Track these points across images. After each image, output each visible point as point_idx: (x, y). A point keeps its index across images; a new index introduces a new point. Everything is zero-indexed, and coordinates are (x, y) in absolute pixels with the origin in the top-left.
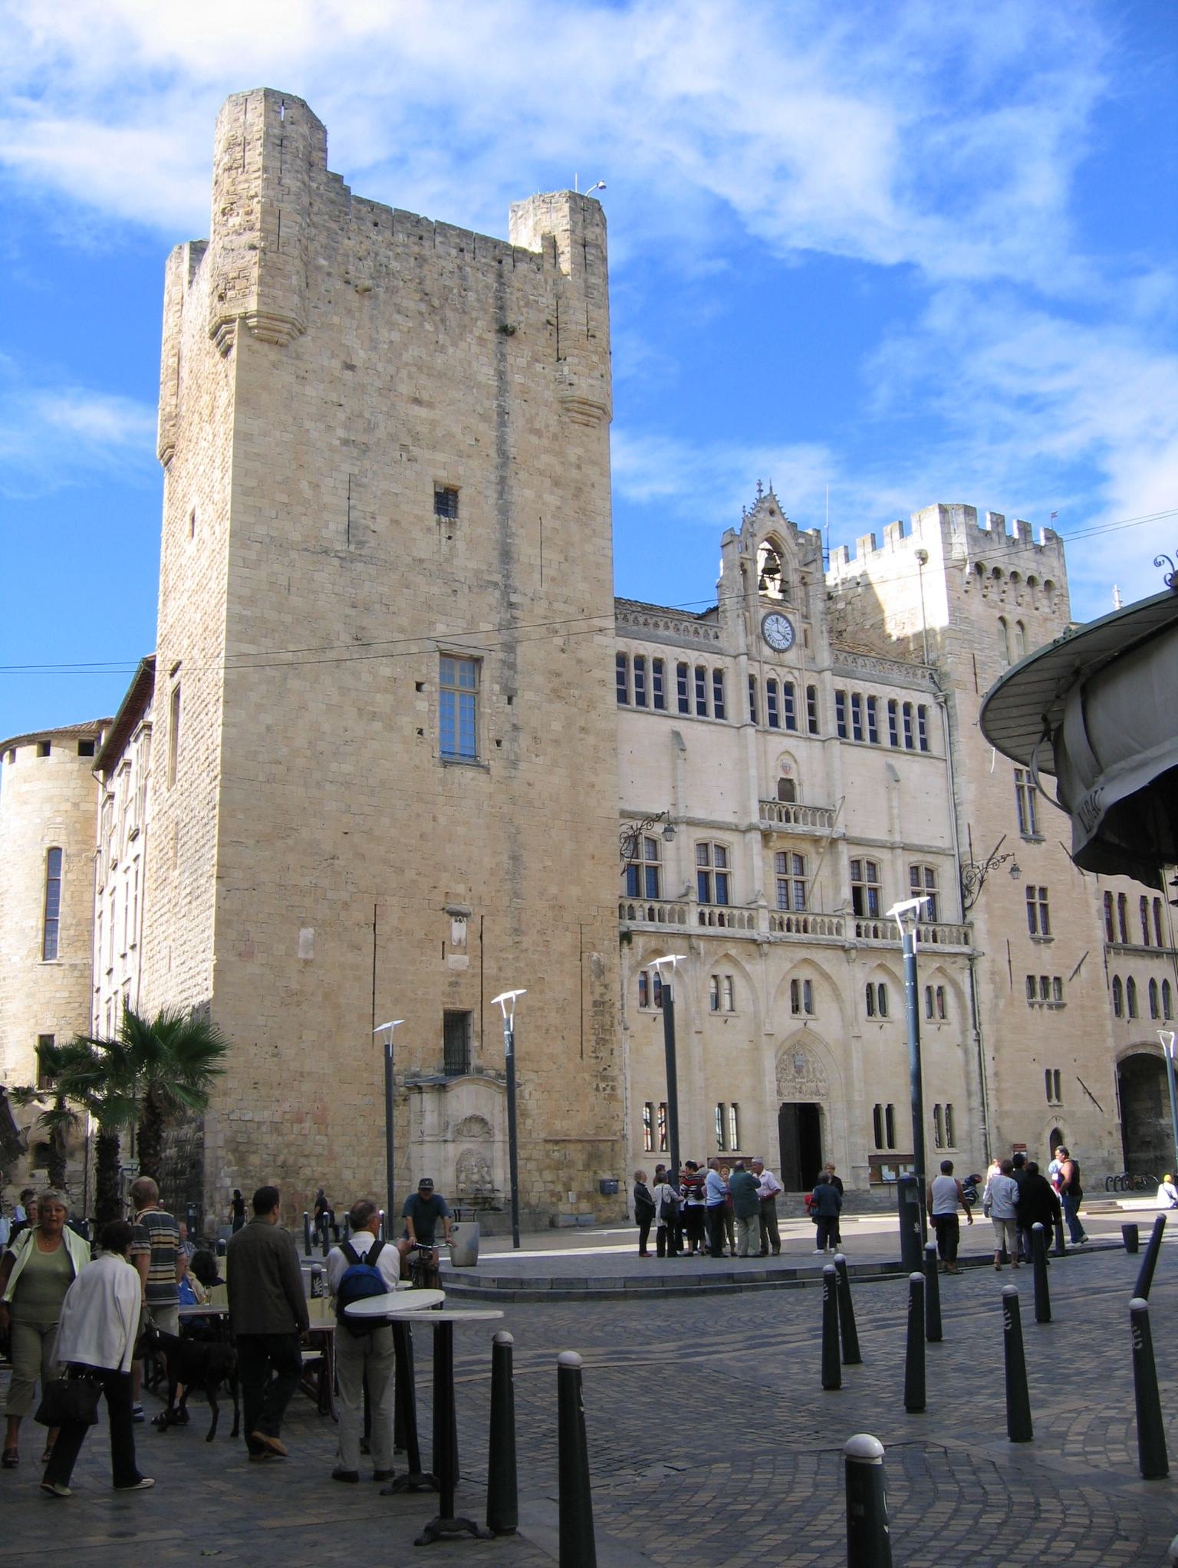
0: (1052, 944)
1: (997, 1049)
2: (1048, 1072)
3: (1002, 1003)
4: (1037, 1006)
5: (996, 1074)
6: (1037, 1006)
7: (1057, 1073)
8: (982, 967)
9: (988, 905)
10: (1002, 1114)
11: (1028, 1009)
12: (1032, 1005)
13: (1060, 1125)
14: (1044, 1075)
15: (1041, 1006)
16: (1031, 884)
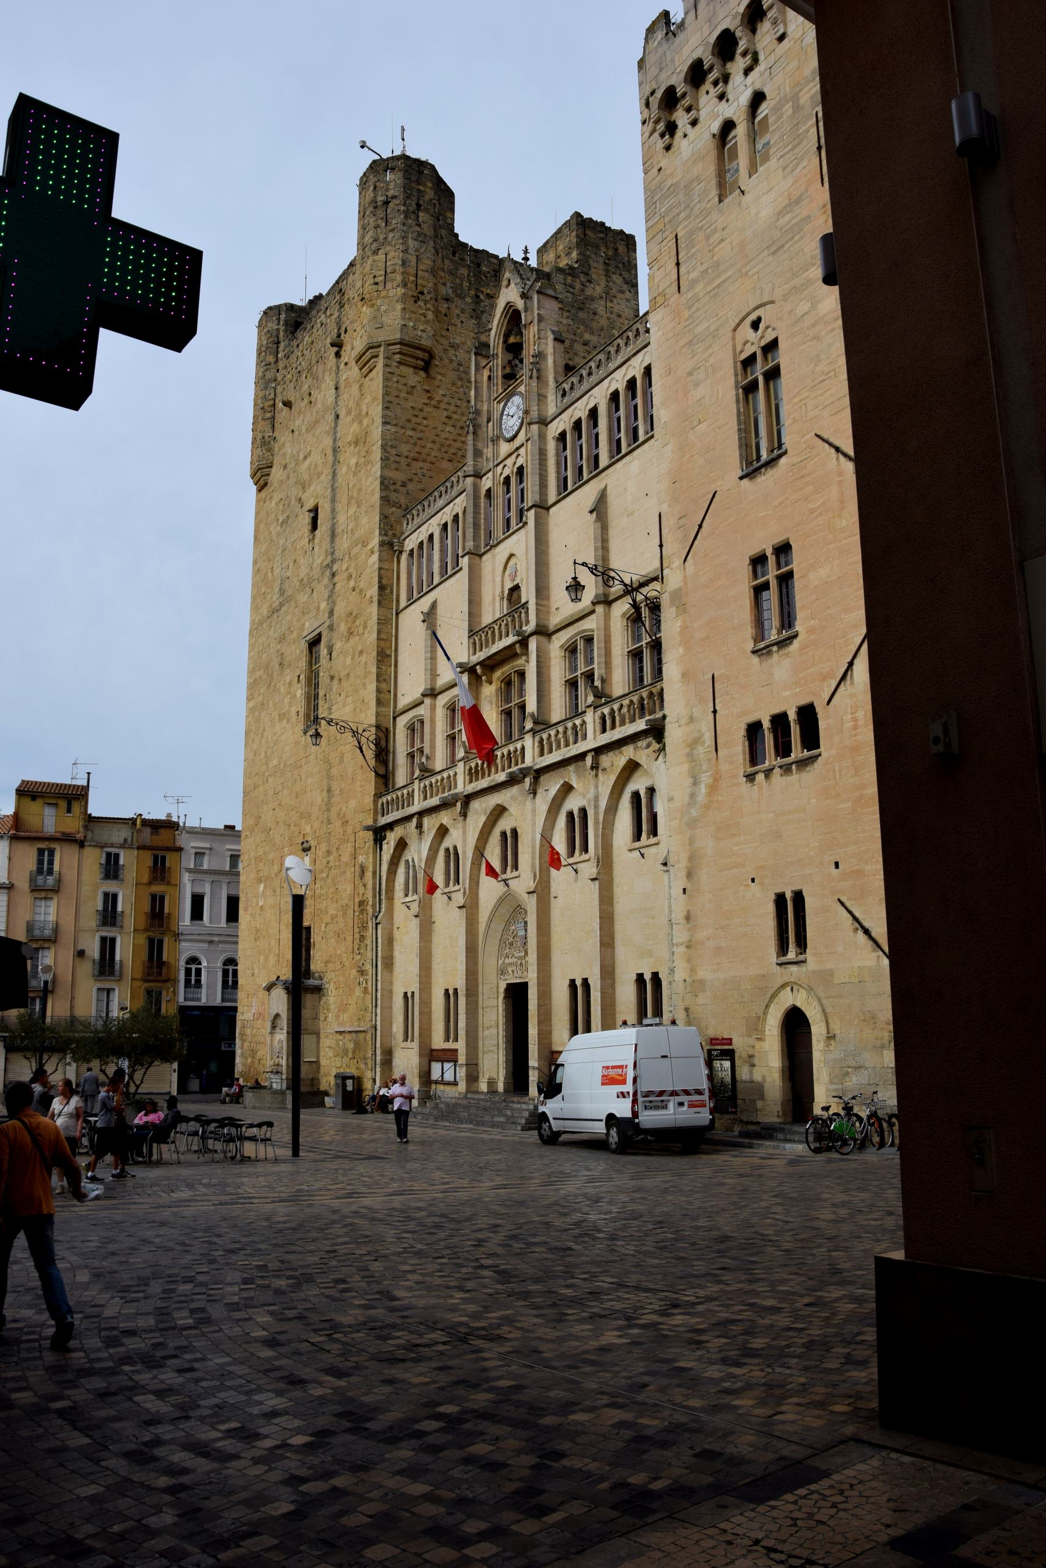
0: (796, 643)
1: (689, 875)
2: (780, 900)
3: (703, 789)
4: (760, 777)
5: (688, 918)
6: (760, 777)
7: (799, 897)
8: (673, 733)
9: (684, 628)
10: (696, 986)
11: (744, 786)
12: (750, 777)
13: (801, 1000)
14: (771, 908)
15: (768, 773)
16: (754, 551)
